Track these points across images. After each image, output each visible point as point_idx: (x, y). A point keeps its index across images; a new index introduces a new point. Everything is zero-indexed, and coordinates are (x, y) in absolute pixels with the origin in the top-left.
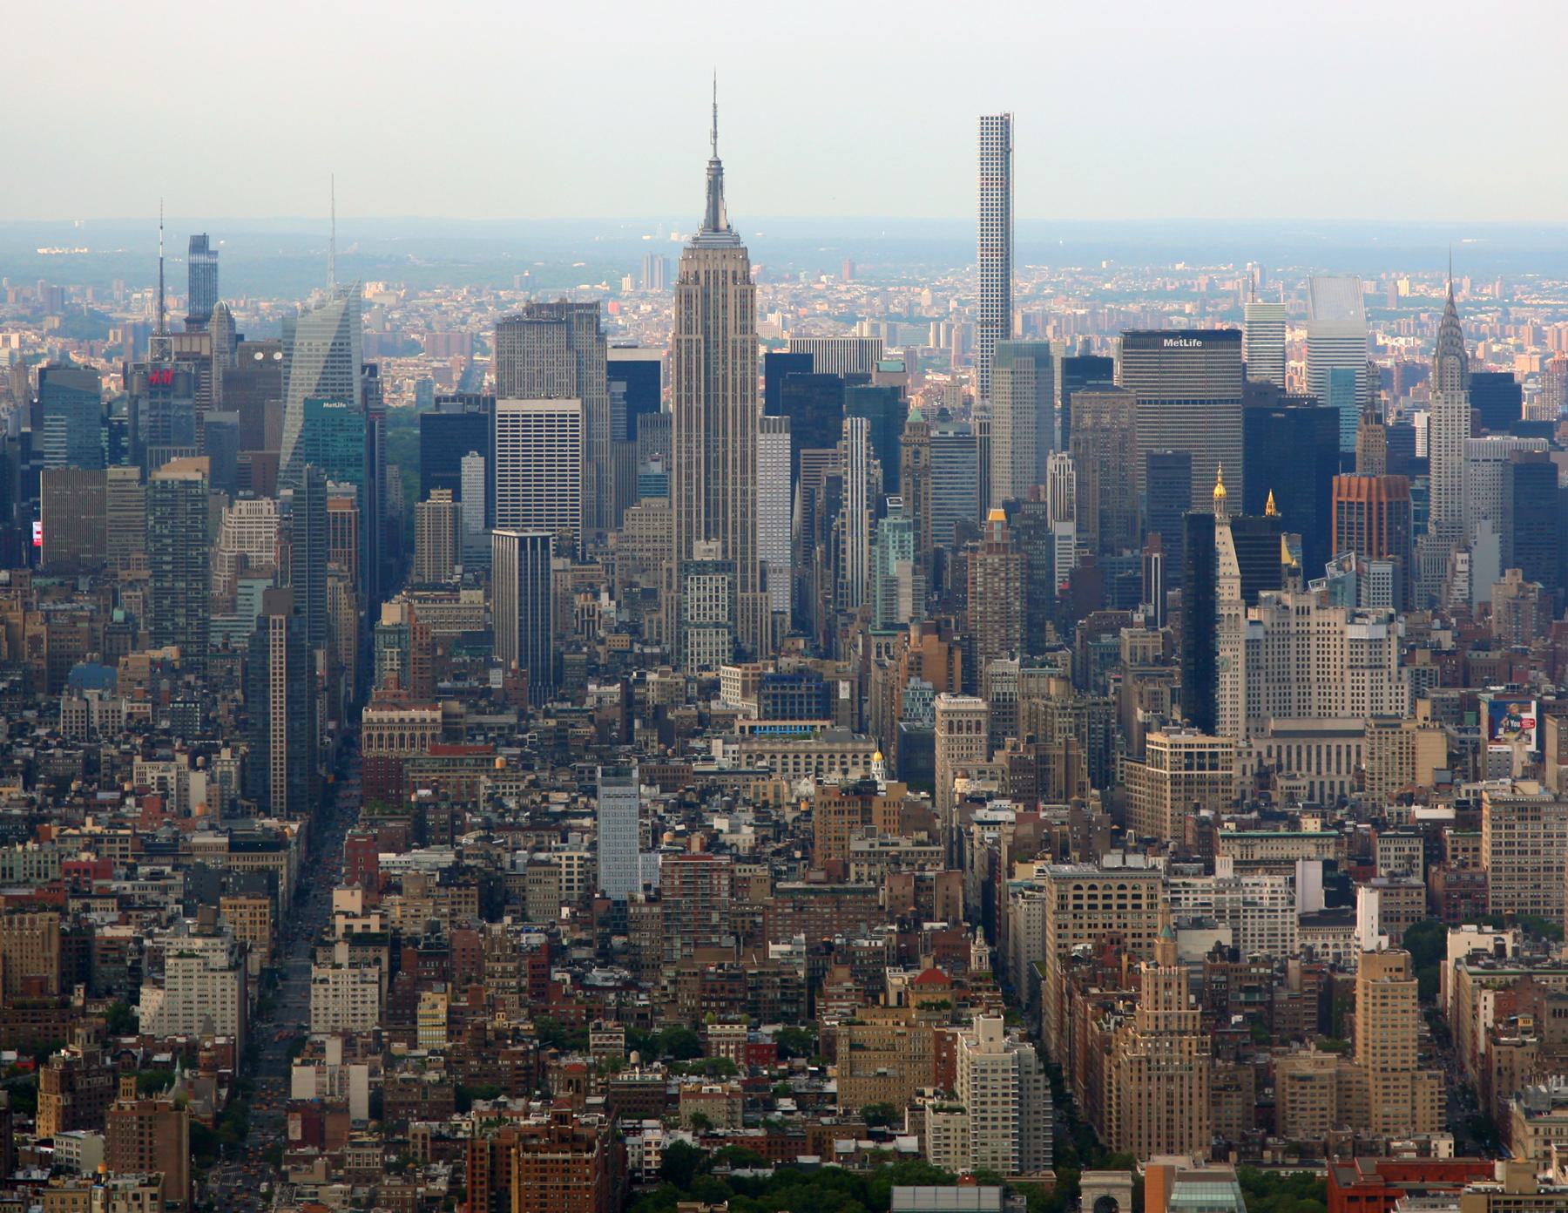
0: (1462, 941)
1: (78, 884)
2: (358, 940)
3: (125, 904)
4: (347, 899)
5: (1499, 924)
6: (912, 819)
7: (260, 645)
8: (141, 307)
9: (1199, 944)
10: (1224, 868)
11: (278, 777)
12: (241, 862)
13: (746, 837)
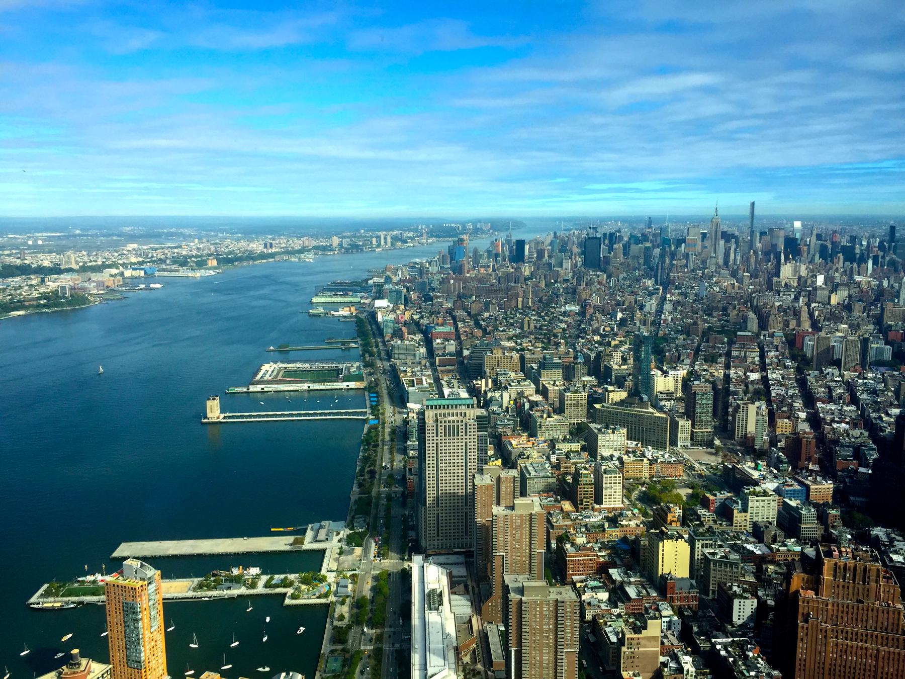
0: (813, 305)
4: (668, 296)
5: (819, 303)
7: (657, 266)
8: (642, 226)
9: (777, 304)
10: (781, 295)
11: (659, 282)
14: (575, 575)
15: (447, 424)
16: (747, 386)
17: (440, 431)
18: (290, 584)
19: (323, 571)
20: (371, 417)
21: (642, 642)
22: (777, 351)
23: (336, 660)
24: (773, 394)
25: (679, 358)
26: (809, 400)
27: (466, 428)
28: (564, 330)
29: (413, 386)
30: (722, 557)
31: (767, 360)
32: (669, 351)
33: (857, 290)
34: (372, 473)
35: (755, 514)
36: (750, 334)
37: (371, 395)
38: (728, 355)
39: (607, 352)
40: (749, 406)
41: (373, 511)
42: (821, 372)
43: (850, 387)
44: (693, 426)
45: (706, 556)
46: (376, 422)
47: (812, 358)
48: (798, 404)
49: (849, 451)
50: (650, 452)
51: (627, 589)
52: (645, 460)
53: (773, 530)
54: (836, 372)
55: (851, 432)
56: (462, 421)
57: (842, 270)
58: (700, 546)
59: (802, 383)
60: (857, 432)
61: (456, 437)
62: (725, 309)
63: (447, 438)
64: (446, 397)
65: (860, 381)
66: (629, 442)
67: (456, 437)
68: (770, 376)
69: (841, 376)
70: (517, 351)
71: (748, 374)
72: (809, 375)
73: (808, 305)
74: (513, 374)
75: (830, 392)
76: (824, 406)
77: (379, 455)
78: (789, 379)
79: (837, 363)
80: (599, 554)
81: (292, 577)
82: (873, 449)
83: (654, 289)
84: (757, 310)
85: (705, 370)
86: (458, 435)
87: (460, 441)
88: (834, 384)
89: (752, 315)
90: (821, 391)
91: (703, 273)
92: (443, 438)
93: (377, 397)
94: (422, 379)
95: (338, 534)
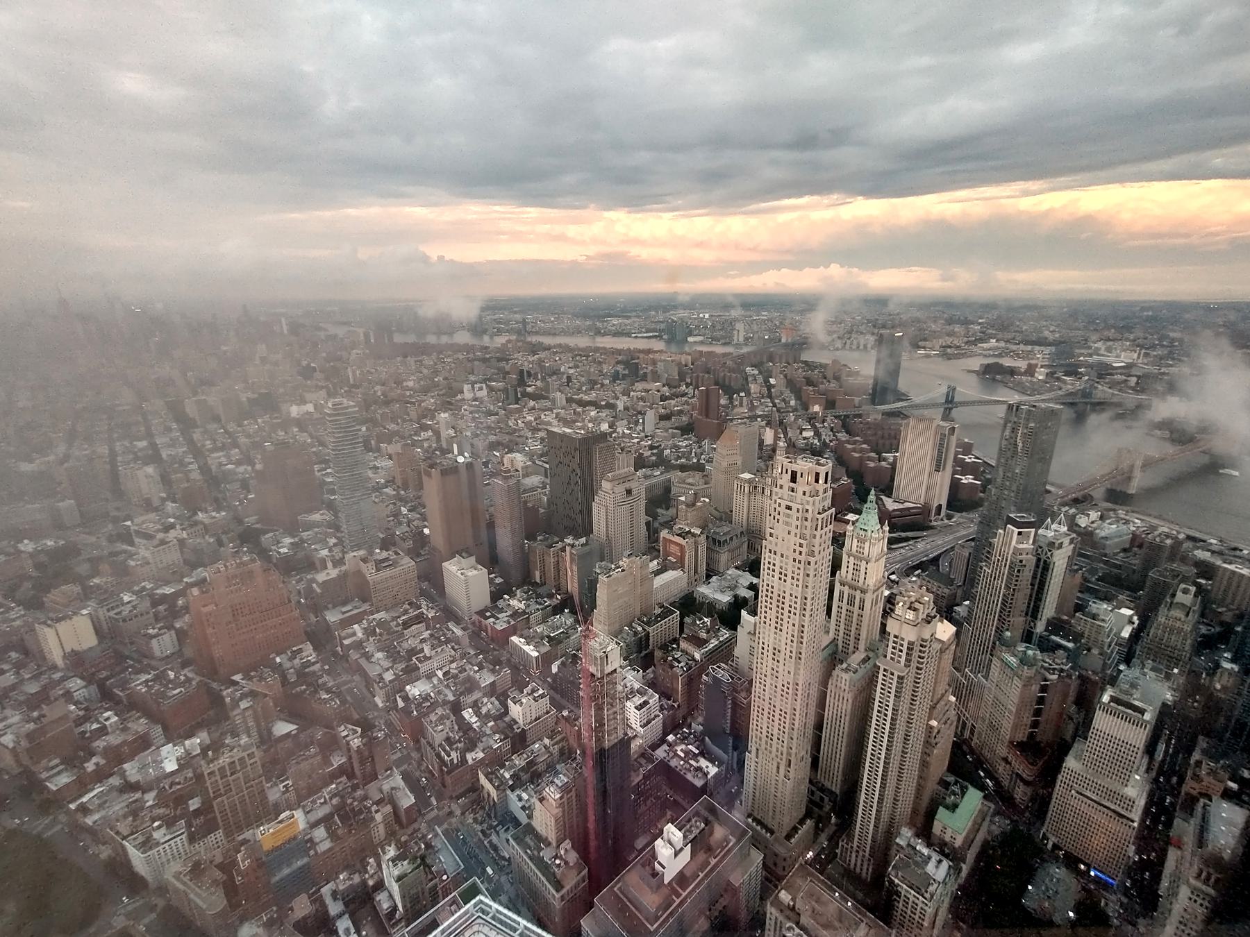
22: (162, 417)
26: (197, 452)
48: (189, 459)
58: (105, 611)
59: (191, 442)
60: (241, 469)
65: (239, 428)
69: (223, 427)
72: (194, 432)
75: (215, 443)
79: (216, 419)
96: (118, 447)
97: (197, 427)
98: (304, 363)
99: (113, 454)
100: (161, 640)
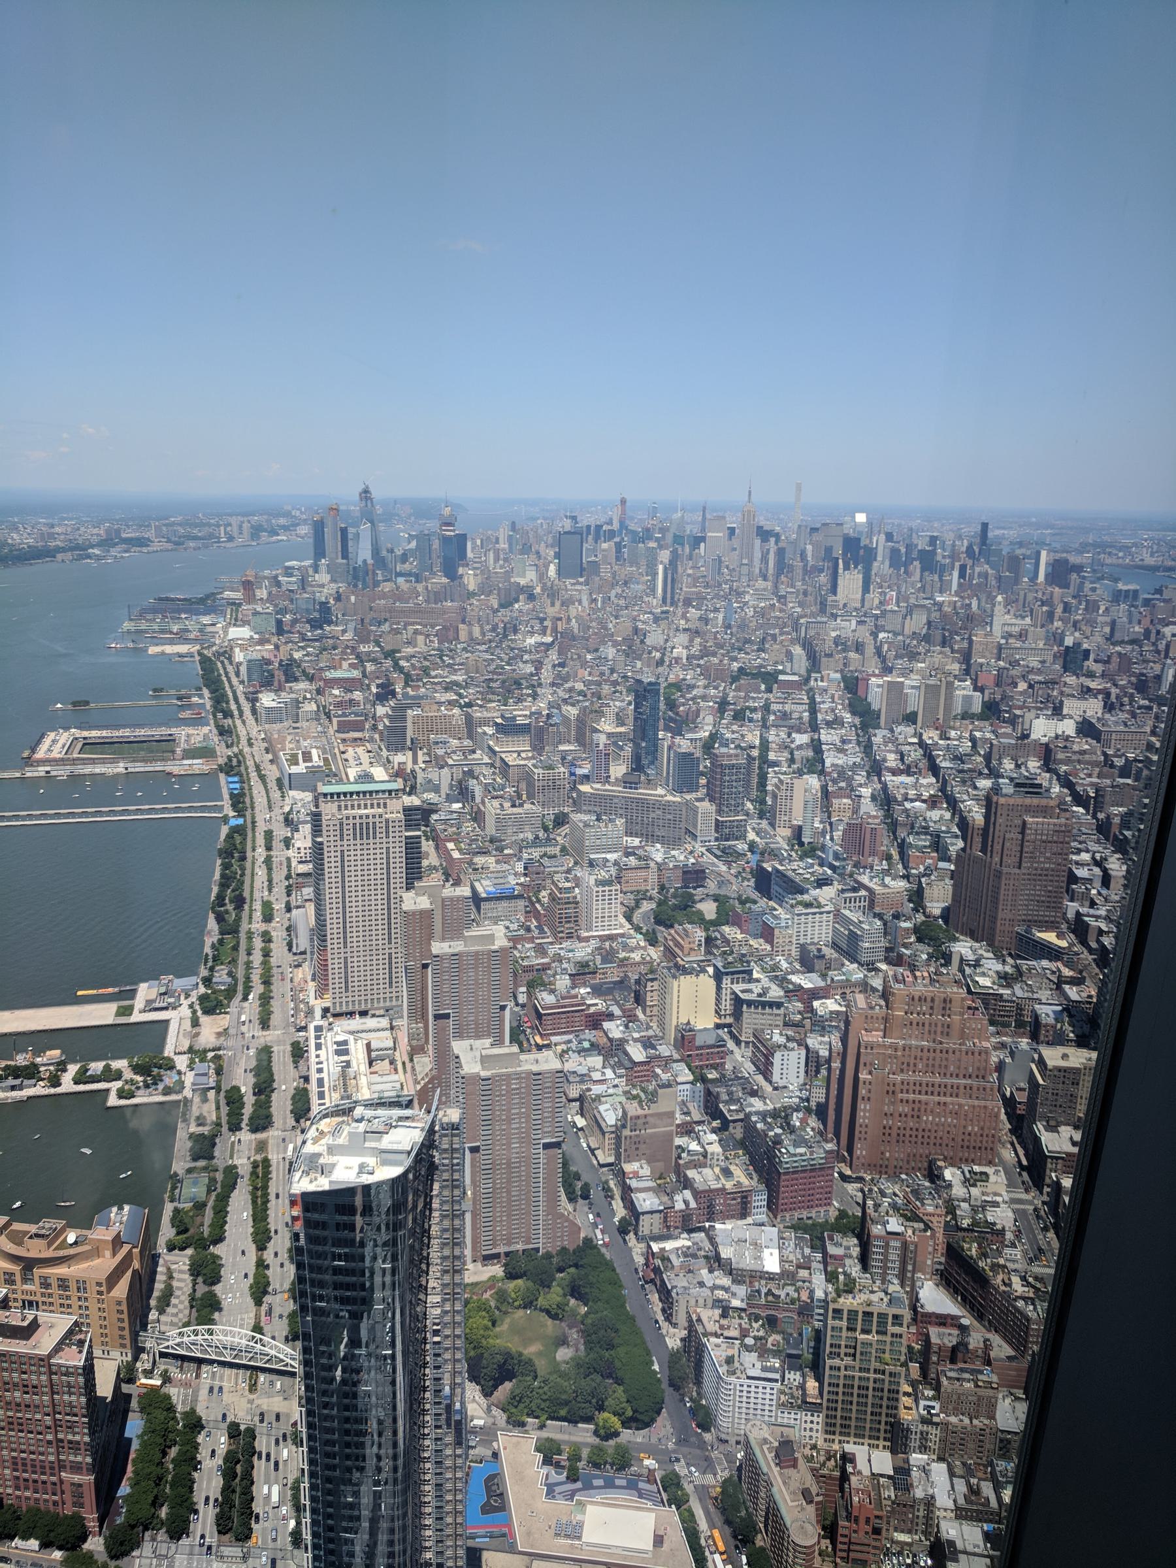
0: (882, 635)
1: (635, 619)
2: (685, 630)
3: (644, 622)
6: (781, 611)
9: (834, 634)
10: (839, 621)
12: (664, 616)
13: (752, 613)
14: (554, 1034)
15: (358, 821)
16: (792, 753)
17: (346, 832)
18: (118, 1075)
19: (168, 1051)
20: (232, 814)
21: (649, 1119)
22: (833, 702)
23: (195, 1183)
24: (828, 763)
25: (698, 716)
26: (876, 769)
27: (387, 827)
28: (532, 675)
29: (297, 764)
30: (760, 995)
31: (820, 716)
32: (683, 705)
33: (938, 614)
34: (239, 902)
35: (802, 933)
36: (796, 678)
37: (230, 779)
38: (766, 708)
39: (596, 707)
40: (795, 781)
41: (242, 957)
42: (892, 731)
43: (927, 751)
44: (719, 812)
45: (737, 995)
46: (240, 821)
47: (880, 710)
48: (860, 778)
49: (925, 840)
50: (657, 853)
51: (628, 1049)
52: (652, 864)
53: (828, 952)
54: (910, 730)
55: (929, 814)
56: (380, 816)
57: (919, 585)
59: (868, 748)
61: (371, 841)
62: (763, 640)
63: (358, 842)
64: (352, 779)
65: (941, 742)
66: (629, 839)
67: (371, 841)
68: (823, 738)
70: (461, 707)
71: (794, 735)
72: (875, 735)
73: (875, 635)
74: (455, 742)
75: (902, 759)
76: (894, 778)
77: (248, 872)
78: (850, 741)
79: (911, 718)
80: (588, 1002)
81: (120, 1064)
82: (957, 837)
83: (662, 612)
84: (808, 645)
85: (733, 732)
86: (374, 838)
87: (378, 846)
88: (908, 748)
89: (798, 650)
90: (892, 760)
91: (731, 588)
92: (352, 842)
93: (242, 782)
94: (310, 753)
95: (187, 996)
96: (772, 736)
97: (879, 727)
98: (1069, 641)
99: (765, 746)
100: (785, 1057)
